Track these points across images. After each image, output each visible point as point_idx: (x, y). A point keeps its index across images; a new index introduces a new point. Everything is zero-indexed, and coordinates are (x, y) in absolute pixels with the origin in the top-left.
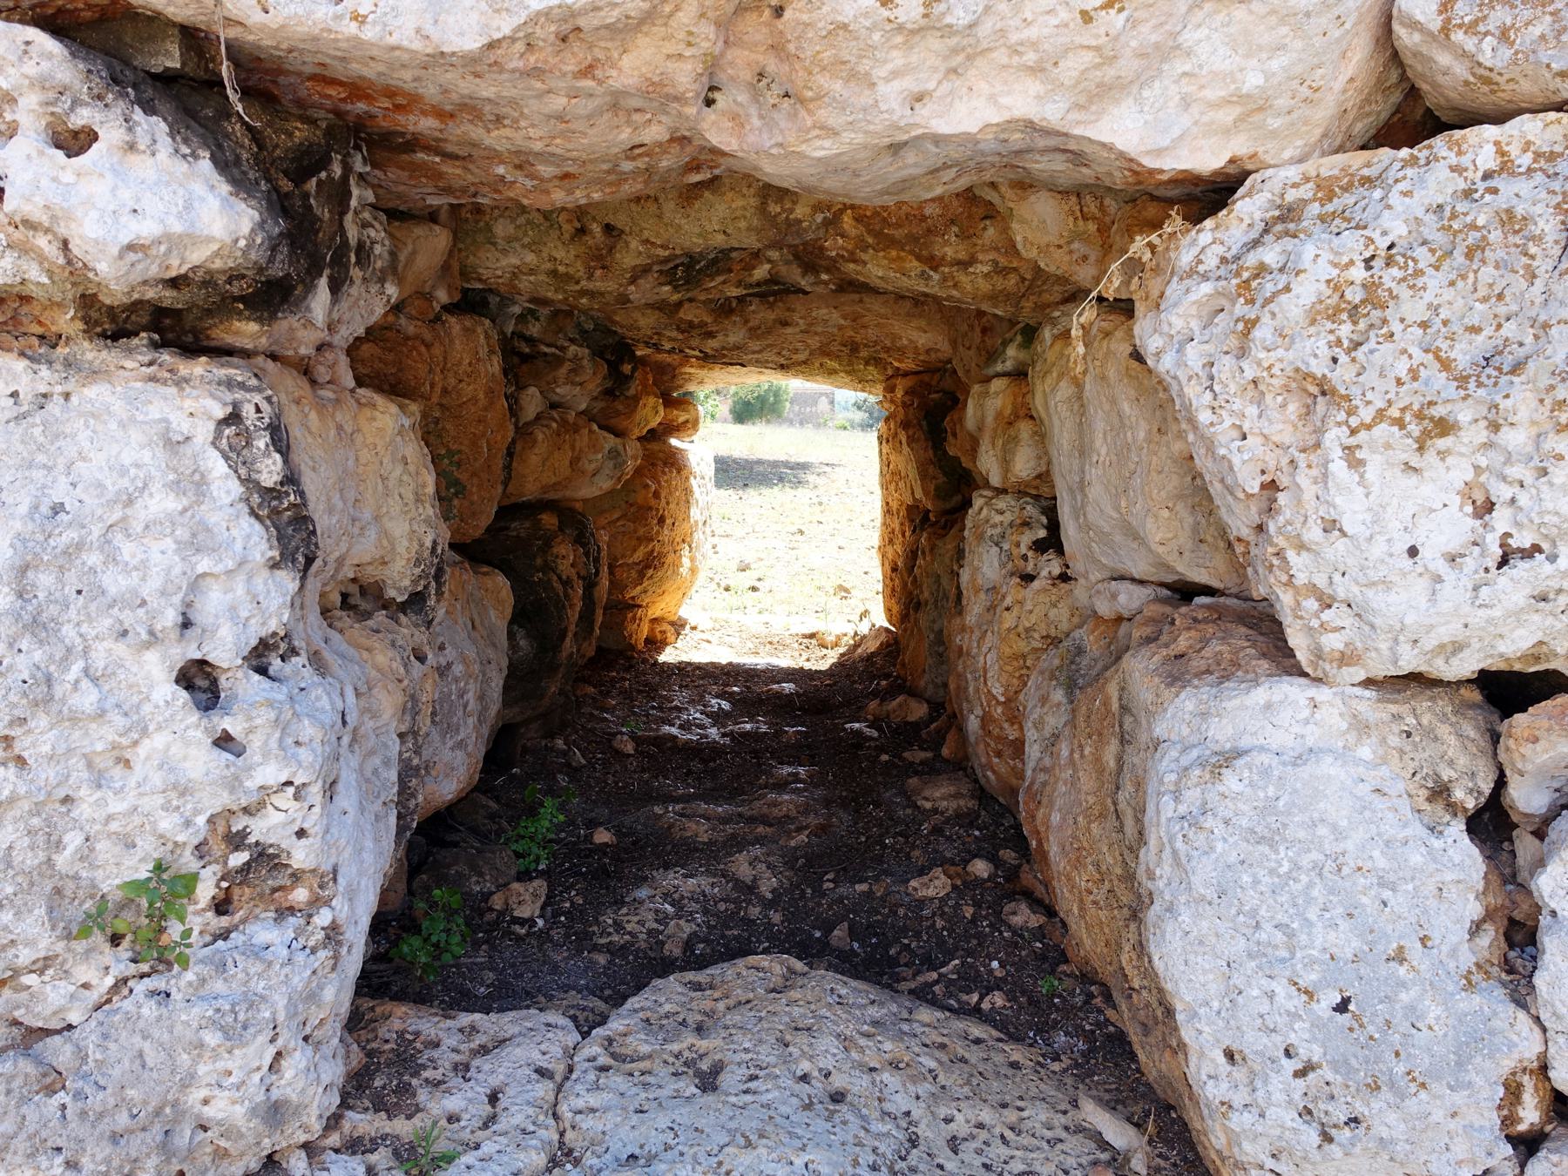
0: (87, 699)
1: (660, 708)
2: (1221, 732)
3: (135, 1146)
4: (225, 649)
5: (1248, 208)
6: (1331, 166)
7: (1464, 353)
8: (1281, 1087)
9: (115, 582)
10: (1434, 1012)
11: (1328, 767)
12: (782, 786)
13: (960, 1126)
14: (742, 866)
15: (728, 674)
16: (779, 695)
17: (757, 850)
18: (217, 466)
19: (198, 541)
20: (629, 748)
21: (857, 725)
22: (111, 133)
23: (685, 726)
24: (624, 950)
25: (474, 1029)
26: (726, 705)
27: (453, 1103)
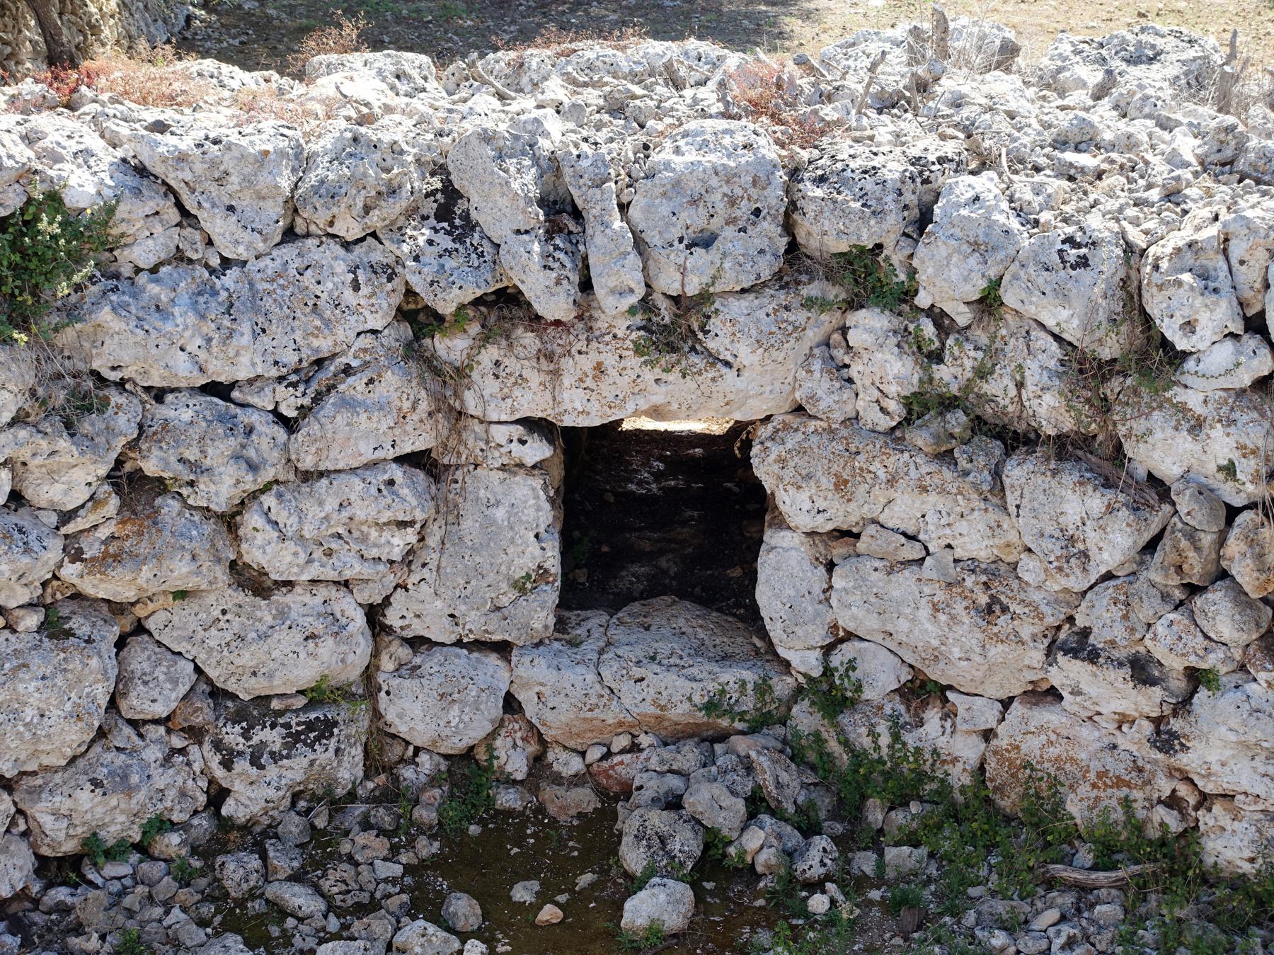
0: (520, 542)
1: (625, 471)
2: (773, 542)
3: (523, 631)
4: (542, 530)
5: (770, 427)
6: (789, 418)
7: (804, 473)
8: (779, 625)
9: (524, 518)
10: (810, 608)
11: (793, 553)
12: (684, 523)
13: (718, 642)
14: (663, 563)
15: (664, 439)
16: (693, 458)
17: (670, 556)
18: (542, 493)
19: (539, 509)
20: (612, 499)
21: (729, 485)
22: (530, 441)
23: (640, 483)
24: (619, 594)
25: (578, 615)
26: (662, 466)
27: (578, 632)
